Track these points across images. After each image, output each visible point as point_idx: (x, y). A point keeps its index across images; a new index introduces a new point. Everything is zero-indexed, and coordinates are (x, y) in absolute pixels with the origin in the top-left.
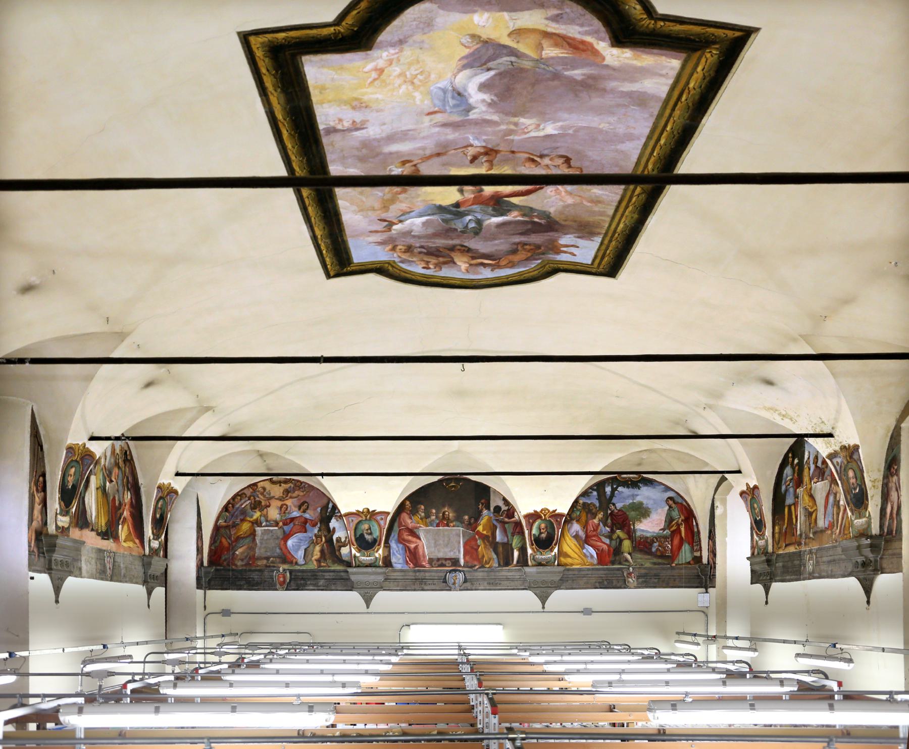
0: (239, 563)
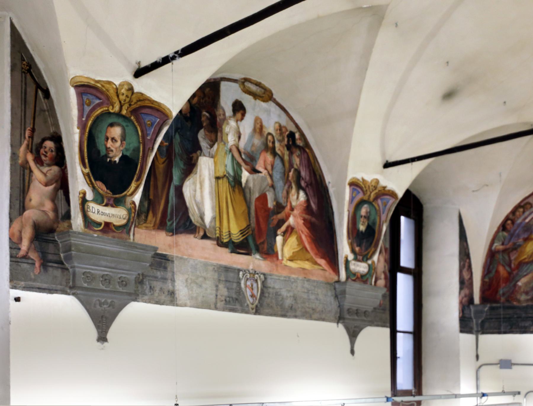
0: (523, 297)
